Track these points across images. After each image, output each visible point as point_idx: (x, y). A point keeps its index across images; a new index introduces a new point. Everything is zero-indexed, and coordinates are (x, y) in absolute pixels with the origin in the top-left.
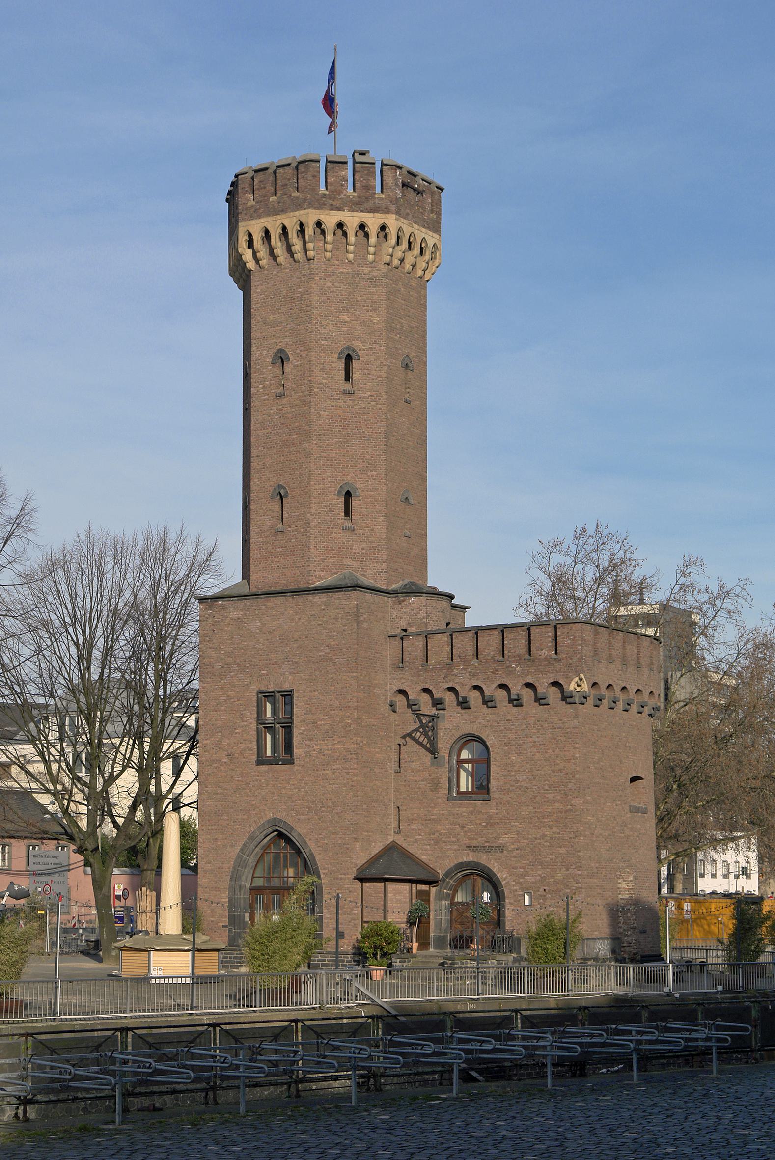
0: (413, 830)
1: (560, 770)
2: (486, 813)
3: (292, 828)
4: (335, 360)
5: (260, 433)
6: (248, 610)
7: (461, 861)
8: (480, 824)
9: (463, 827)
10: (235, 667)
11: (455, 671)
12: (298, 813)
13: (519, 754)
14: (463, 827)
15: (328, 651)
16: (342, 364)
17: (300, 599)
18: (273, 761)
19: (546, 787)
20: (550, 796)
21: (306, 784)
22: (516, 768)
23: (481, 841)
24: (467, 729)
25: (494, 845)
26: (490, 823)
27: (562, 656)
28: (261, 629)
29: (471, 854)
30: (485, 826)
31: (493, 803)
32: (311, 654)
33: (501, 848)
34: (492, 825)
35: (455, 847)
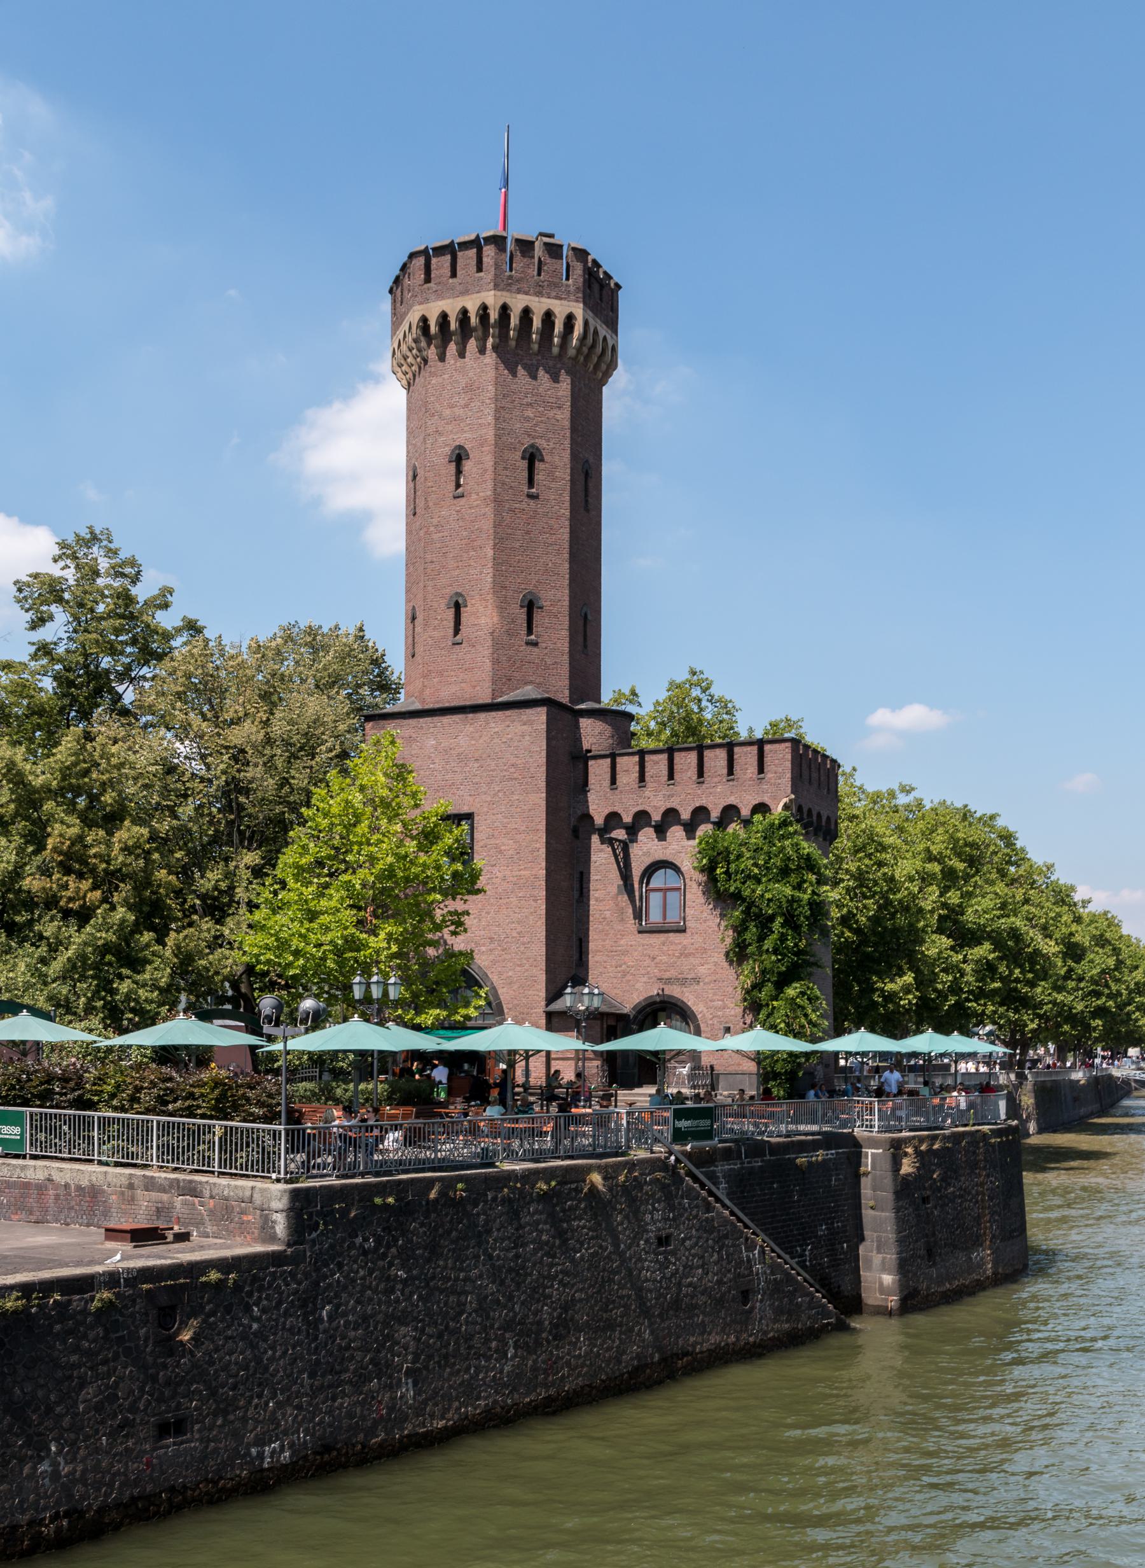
16: (525, 464)
21: (488, 913)
25: (690, 977)
26: (684, 954)
27: (769, 775)
32: (494, 774)
33: (697, 980)
34: (687, 956)
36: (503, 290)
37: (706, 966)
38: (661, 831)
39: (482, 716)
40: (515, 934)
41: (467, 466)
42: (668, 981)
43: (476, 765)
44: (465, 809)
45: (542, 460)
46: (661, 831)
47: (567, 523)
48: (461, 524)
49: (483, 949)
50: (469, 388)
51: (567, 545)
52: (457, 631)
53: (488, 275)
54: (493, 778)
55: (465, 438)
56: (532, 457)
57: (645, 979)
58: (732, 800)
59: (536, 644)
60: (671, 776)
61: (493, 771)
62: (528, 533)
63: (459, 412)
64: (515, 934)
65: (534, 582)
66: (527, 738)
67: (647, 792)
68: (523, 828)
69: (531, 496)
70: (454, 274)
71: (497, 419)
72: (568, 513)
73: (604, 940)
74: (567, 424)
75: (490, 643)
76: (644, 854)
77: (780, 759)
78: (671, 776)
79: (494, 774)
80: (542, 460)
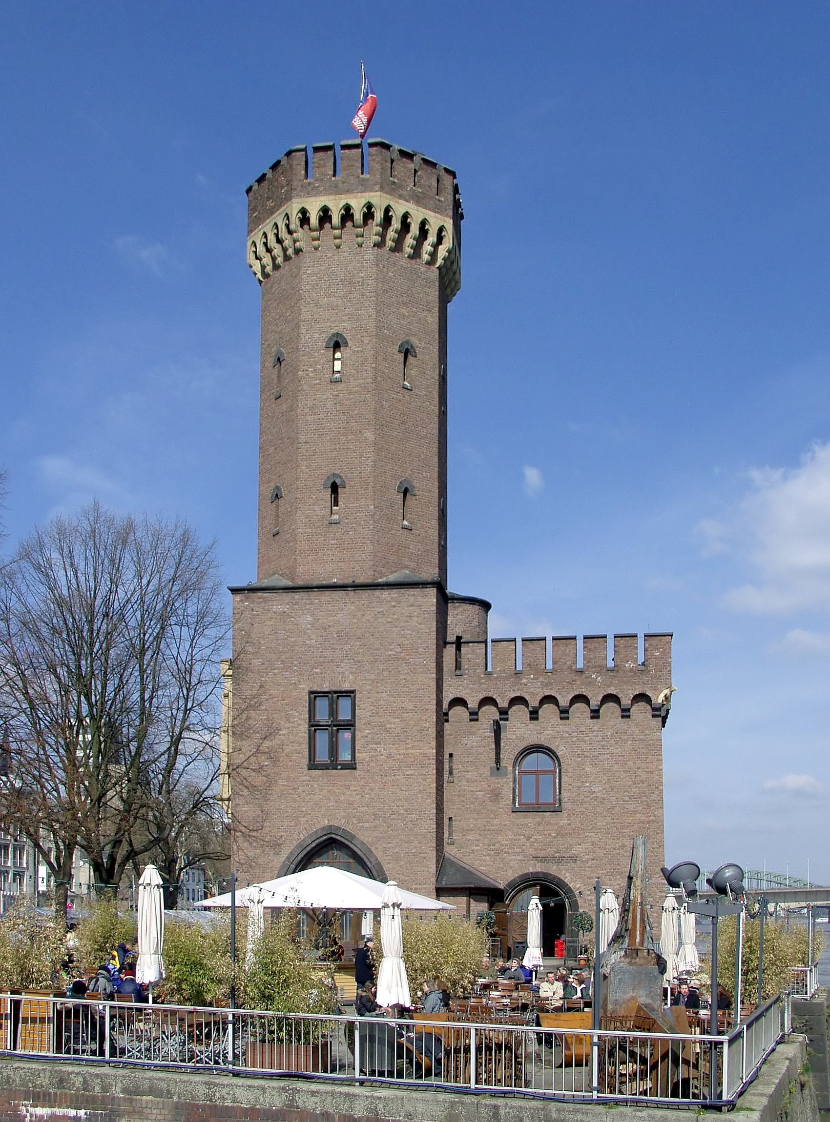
0: (469, 840)
1: (642, 782)
2: (556, 824)
3: (353, 837)
4: (397, 352)
5: (309, 418)
6: (297, 603)
7: (527, 871)
8: (550, 835)
9: (528, 838)
10: (279, 664)
11: (524, 681)
12: (360, 820)
13: (595, 765)
14: (528, 838)
15: (399, 650)
17: (365, 594)
18: (325, 767)
19: (627, 798)
20: (631, 807)
21: (372, 790)
22: (591, 779)
23: (550, 851)
24: (534, 740)
25: (567, 855)
28: (313, 625)
29: (539, 865)
30: (555, 837)
31: (565, 814)
32: (379, 653)
33: (574, 859)
35: (519, 858)
40: (402, 811)
42: (544, 859)
43: (358, 643)
44: (346, 687)
49: (367, 825)
55: (343, 327)
64: (402, 811)
73: (476, 819)
76: (518, 738)
79: (379, 653)
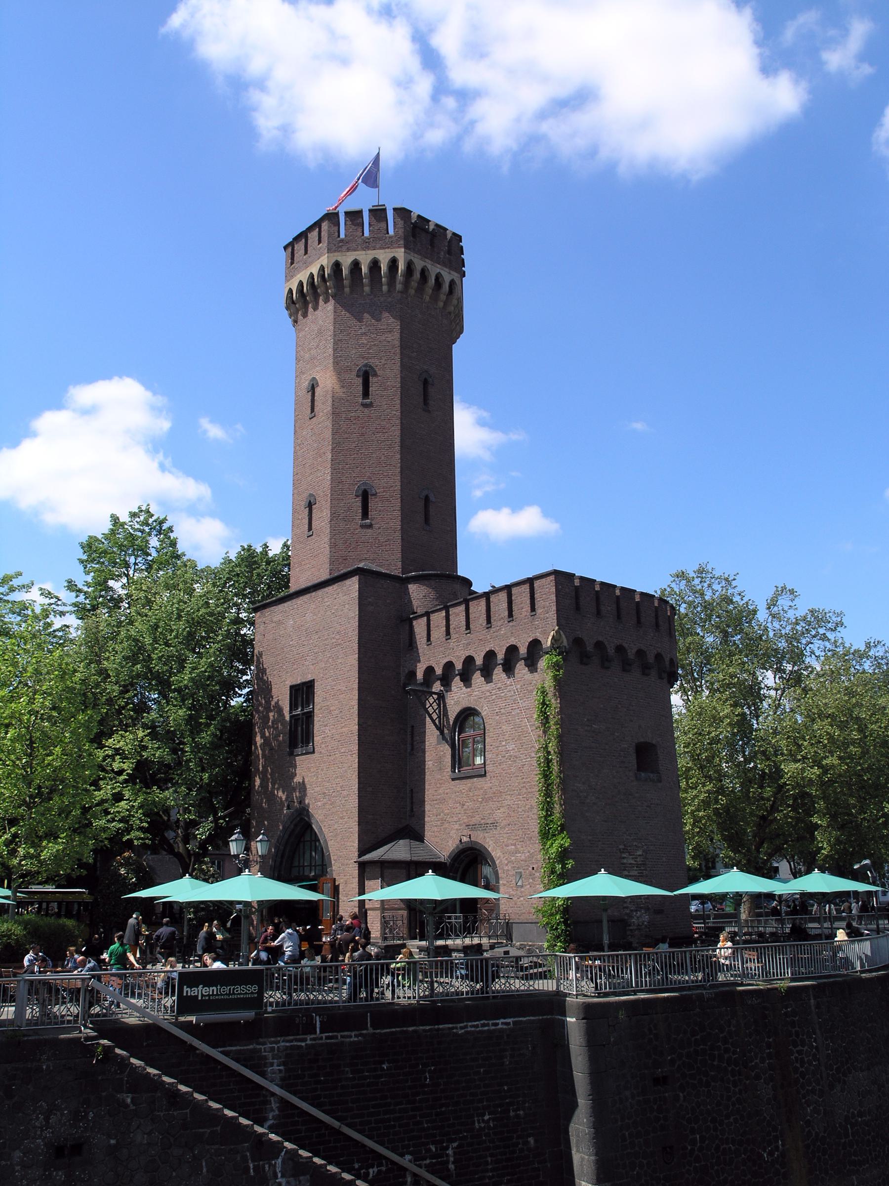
2: (481, 788)
16: (360, 381)
22: (506, 737)
23: (476, 819)
27: (539, 611)
30: (481, 803)
33: (494, 825)
36: (335, 251)
37: (502, 810)
38: (466, 679)
39: (320, 592)
40: (339, 789)
41: (318, 391)
45: (376, 375)
46: (466, 679)
47: (398, 421)
48: (314, 438)
50: (320, 332)
51: (398, 440)
52: (310, 529)
53: (324, 245)
54: (314, 646)
56: (366, 376)
57: (457, 827)
58: (512, 641)
59: (370, 526)
60: (468, 627)
61: (326, 640)
62: (363, 435)
63: (313, 352)
64: (339, 789)
65: (368, 474)
66: (347, 606)
67: (452, 643)
68: (344, 688)
69: (365, 405)
70: (306, 253)
71: (335, 350)
72: (398, 413)
74: (397, 343)
75: (328, 531)
77: (547, 593)
78: (468, 627)
80: (376, 375)
